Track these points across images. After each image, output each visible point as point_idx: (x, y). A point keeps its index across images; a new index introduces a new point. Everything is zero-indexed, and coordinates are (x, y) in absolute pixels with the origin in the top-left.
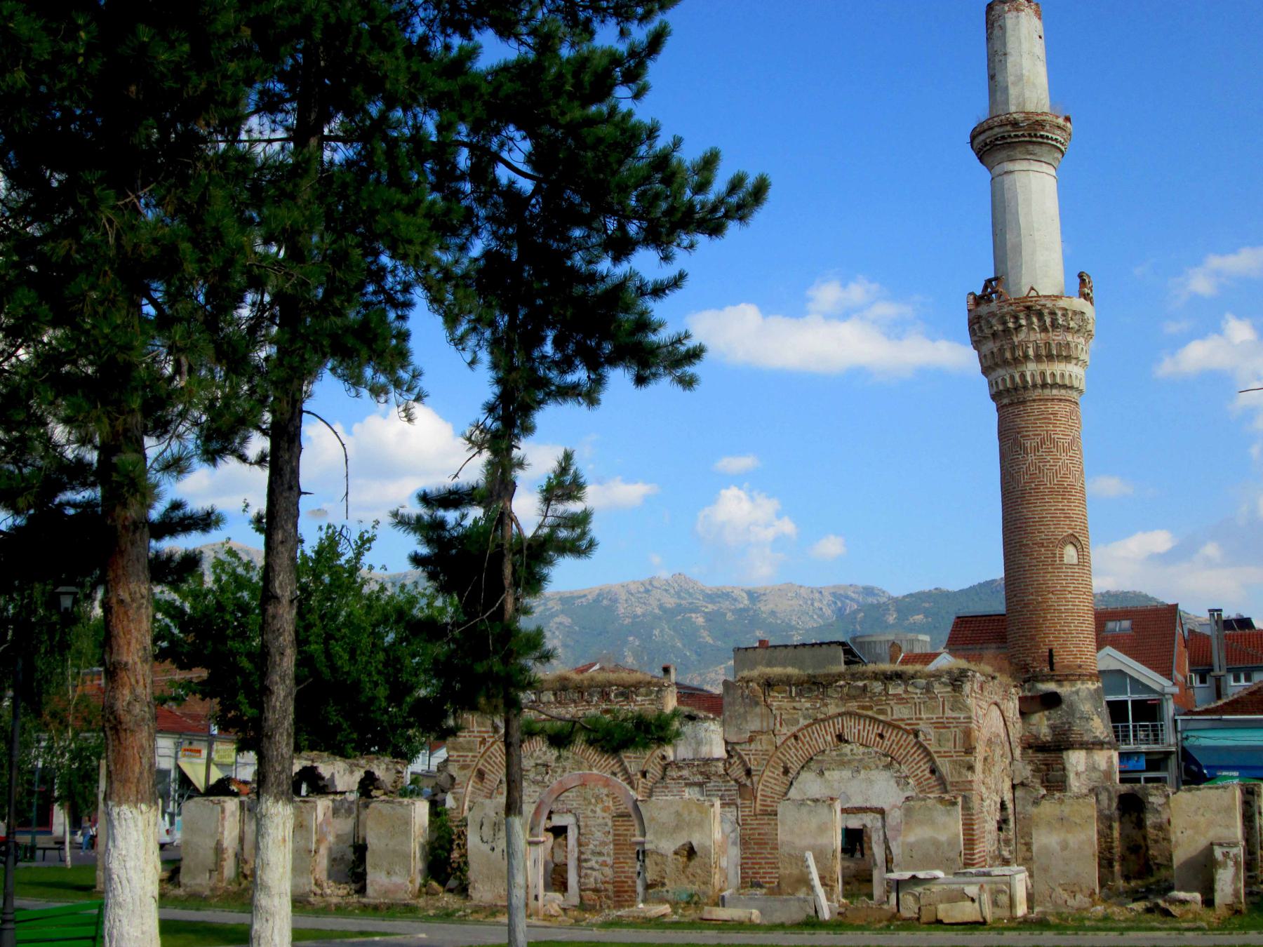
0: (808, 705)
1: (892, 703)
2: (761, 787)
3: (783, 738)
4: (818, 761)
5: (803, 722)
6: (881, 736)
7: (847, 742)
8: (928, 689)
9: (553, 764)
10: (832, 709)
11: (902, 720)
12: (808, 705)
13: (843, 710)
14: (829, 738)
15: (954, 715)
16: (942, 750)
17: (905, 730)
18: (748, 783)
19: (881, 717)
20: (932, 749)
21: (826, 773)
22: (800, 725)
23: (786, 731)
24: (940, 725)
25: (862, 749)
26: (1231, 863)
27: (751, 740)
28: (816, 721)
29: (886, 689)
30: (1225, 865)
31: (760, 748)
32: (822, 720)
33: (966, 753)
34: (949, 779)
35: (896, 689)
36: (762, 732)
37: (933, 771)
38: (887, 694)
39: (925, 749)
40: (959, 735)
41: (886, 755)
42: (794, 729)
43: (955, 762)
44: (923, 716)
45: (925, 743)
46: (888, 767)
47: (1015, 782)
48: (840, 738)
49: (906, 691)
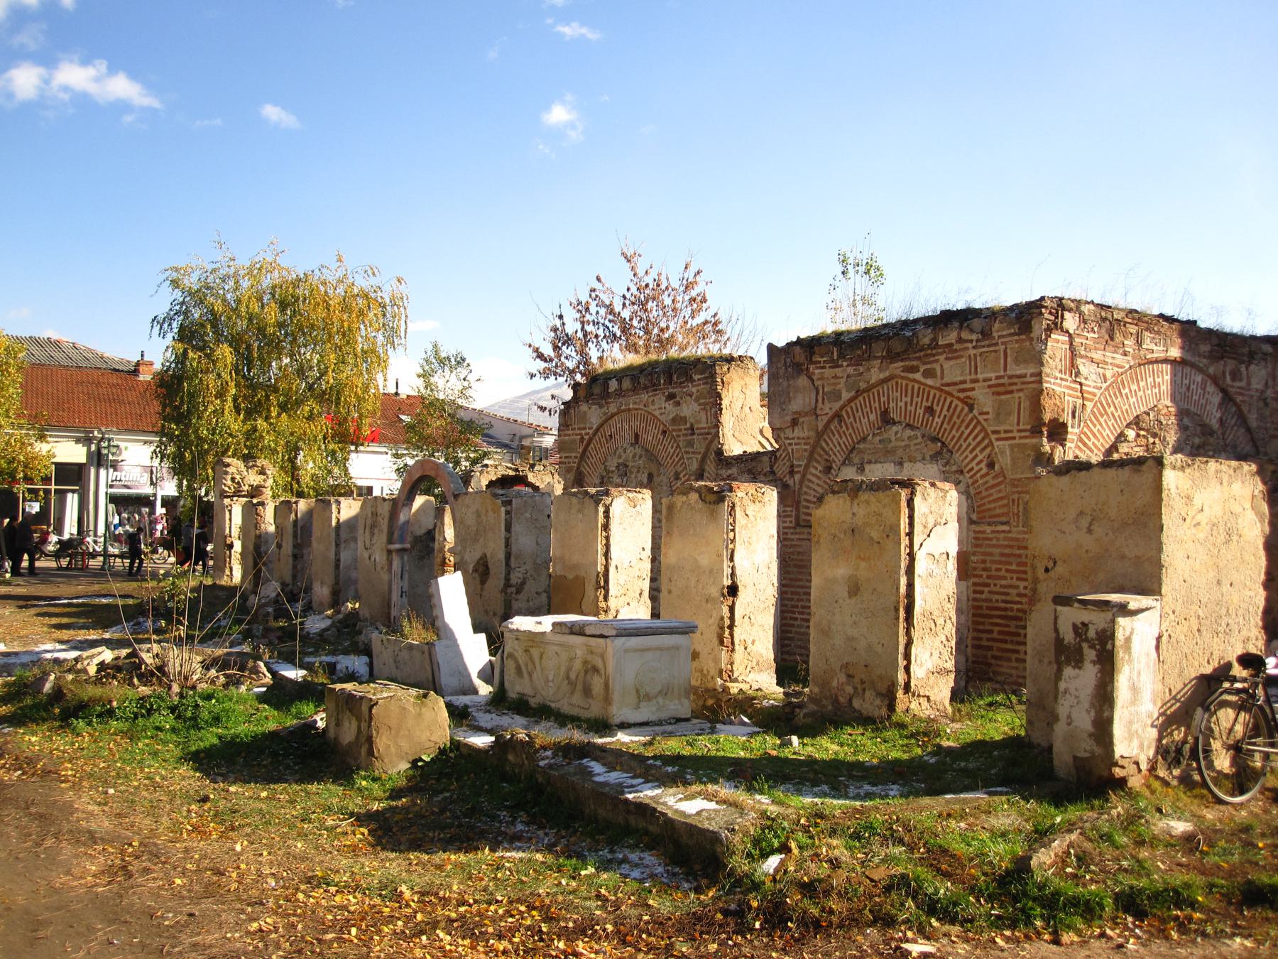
0: (850, 370)
1: (942, 358)
2: (805, 489)
3: (825, 419)
4: (861, 452)
5: (846, 396)
6: (930, 410)
7: (894, 423)
8: (986, 334)
9: (631, 464)
10: (875, 375)
11: (955, 384)
13: (887, 374)
14: (872, 417)
15: (1018, 372)
16: (1001, 428)
17: (958, 398)
18: (791, 482)
20: (989, 429)
21: (867, 467)
22: (841, 403)
23: (829, 408)
24: (1000, 389)
25: (908, 432)
26: (1090, 654)
27: (794, 423)
28: (859, 393)
29: (935, 339)
30: (1078, 662)
31: (802, 435)
32: (867, 390)
34: (1010, 476)
35: (950, 337)
36: (806, 414)
37: (991, 465)
39: (983, 429)
40: (1025, 404)
41: (935, 439)
42: (837, 406)
43: (1018, 445)
44: (980, 376)
45: (981, 418)
46: (935, 457)
49: (960, 340)
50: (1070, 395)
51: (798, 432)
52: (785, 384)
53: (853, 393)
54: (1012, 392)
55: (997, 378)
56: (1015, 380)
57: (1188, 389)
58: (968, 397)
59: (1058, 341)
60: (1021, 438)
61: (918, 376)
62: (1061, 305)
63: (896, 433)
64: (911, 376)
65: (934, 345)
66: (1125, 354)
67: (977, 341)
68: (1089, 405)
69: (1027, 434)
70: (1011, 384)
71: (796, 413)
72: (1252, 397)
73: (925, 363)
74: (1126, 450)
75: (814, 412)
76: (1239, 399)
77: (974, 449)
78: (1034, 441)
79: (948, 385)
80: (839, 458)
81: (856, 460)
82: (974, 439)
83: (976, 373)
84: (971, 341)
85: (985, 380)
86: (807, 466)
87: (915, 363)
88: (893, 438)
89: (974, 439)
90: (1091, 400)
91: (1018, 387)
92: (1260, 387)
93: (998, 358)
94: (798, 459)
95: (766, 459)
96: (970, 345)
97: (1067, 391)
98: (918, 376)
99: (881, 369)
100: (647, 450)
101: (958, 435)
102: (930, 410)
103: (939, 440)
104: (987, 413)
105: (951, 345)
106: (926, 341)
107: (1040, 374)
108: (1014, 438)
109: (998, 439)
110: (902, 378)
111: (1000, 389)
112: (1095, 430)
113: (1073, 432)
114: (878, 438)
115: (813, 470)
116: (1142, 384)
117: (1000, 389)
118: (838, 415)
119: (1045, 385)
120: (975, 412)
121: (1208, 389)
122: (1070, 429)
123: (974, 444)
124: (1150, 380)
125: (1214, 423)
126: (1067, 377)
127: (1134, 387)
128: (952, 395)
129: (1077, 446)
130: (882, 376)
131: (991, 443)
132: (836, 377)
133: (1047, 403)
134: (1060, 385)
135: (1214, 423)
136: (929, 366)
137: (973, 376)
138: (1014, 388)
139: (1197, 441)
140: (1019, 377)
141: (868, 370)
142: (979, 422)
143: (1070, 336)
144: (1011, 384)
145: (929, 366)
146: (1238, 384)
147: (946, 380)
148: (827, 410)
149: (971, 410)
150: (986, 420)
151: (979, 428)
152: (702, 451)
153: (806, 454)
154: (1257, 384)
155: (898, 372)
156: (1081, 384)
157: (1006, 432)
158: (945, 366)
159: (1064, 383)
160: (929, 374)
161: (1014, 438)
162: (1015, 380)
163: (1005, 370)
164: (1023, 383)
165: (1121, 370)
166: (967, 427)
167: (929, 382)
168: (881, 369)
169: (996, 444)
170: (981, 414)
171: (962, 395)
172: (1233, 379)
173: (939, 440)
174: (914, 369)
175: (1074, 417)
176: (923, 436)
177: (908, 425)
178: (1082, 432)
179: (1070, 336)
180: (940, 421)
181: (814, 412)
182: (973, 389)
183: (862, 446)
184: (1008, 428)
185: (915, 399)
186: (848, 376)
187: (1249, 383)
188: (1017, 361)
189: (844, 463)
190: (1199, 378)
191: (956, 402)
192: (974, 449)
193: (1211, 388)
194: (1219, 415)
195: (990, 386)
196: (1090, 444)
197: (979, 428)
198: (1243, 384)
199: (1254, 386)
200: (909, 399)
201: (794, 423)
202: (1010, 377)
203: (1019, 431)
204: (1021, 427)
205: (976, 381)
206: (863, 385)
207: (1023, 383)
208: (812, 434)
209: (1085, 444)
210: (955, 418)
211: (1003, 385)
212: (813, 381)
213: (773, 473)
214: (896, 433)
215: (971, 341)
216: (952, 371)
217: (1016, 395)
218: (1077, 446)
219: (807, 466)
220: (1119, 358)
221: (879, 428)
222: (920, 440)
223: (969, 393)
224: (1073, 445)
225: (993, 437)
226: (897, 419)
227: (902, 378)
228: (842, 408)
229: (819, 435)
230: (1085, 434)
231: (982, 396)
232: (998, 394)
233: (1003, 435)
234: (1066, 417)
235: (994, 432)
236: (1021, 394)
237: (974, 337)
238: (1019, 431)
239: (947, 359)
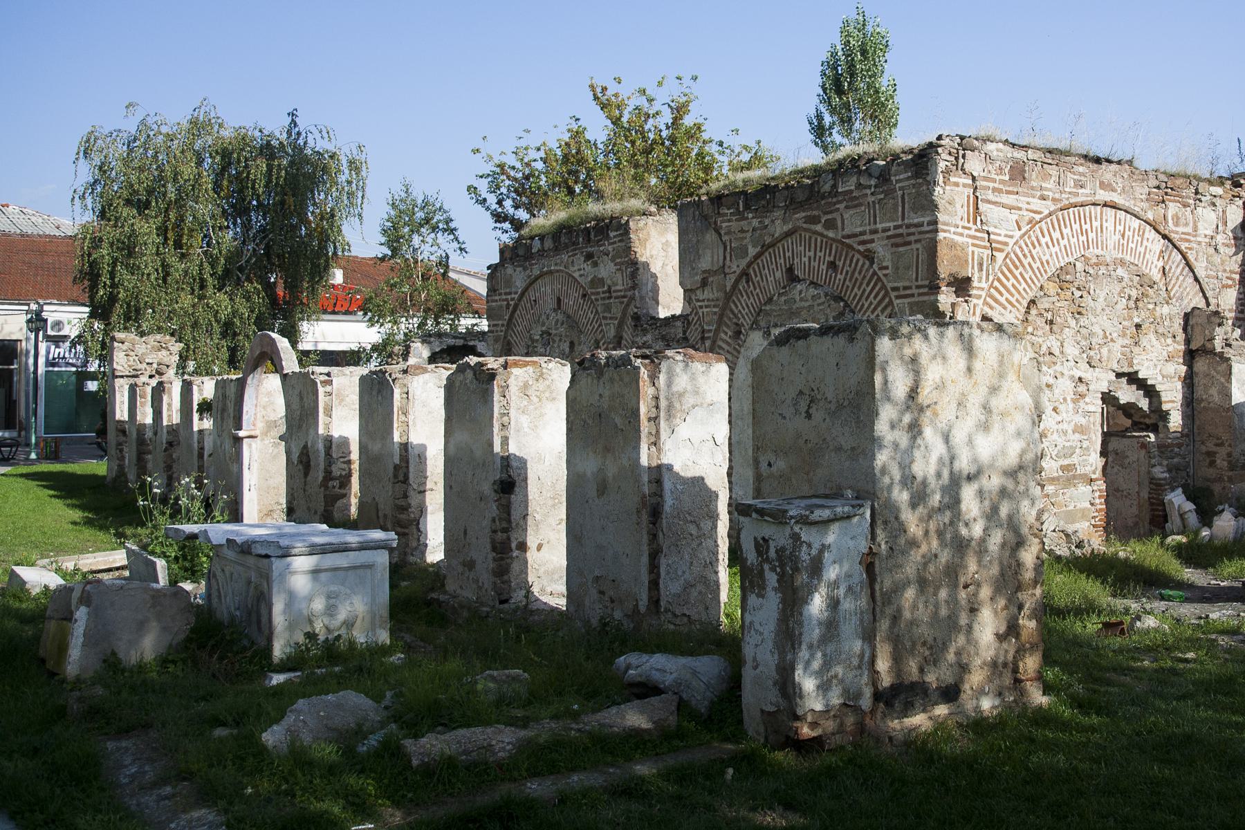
0: (755, 223)
3: (733, 278)
4: (768, 314)
5: (752, 252)
6: (832, 265)
7: (799, 281)
10: (779, 228)
11: (855, 235)
12: (755, 223)
14: (778, 274)
15: (916, 221)
17: (859, 251)
19: (831, 234)
20: (889, 286)
23: (736, 266)
24: (898, 241)
25: (812, 292)
28: (765, 247)
29: (834, 186)
32: (772, 245)
33: (931, 288)
35: (849, 185)
38: (837, 194)
39: (884, 287)
41: (838, 299)
42: (743, 263)
45: (880, 273)
47: (1193, 347)
48: (792, 277)
49: (859, 186)
50: (973, 245)
51: (707, 294)
52: (694, 240)
53: (758, 249)
54: (909, 243)
55: (896, 227)
56: (912, 230)
57: (1123, 236)
58: (868, 250)
59: (957, 184)
60: (920, 295)
61: (819, 228)
62: (964, 145)
63: (801, 292)
64: (812, 227)
65: (834, 192)
66: (1043, 198)
67: (876, 186)
68: (1000, 256)
69: (926, 290)
70: (909, 234)
71: (704, 272)
72: (1199, 243)
73: (825, 213)
74: (1047, 306)
75: (722, 270)
76: (1183, 246)
77: (875, 309)
78: (932, 298)
79: (849, 237)
80: (746, 322)
81: (763, 324)
82: (875, 297)
83: (875, 223)
84: (870, 187)
85: (885, 230)
86: (717, 331)
87: (816, 213)
88: (798, 298)
89: (875, 297)
90: (1002, 251)
91: (917, 237)
92: (1209, 232)
93: (896, 205)
94: (709, 324)
95: (679, 324)
96: (868, 192)
97: (970, 241)
98: (819, 228)
99: (784, 221)
100: (569, 317)
101: (859, 293)
102: (832, 265)
103: (842, 300)
104: (887, 268)
105: (851, 191)
106: (827, 187)
107: (935, 222)
108: (913, 295)
109: (897, 297)
110: (806, 230)
111: (899, 240)
112: (1009, 285)
113: (980, 284)
114: (783, 298)
115: (723, 335)
116: (1066, 231)
117: (899, 240)
118: (745, 274)
119: (941, 235)
120: (875, 266)
121: (1146, 235)
122: (975, 284)
123: (875, 302)
124: (1076, 227)
125: (1156, 275)
126: (971, 225)
127: (1056, 235)
128: (853, 249)
129: (985, 303)
130: (785, 228)
131: (891, 303)
132: (742, 231)
133: (943, 253)
134: (962, 235)
135: (1156, 275)
136: (829, 217)
137: (873, 227)
138: (912, 238)
139: (1134, 293)
140: (916, 226)
141: (773, 221)
142: (879, 279)
143: (974, 179)
144: (909, 234)
145: (829, 217)
146: (1180, 229)
147: (847, 232)
148: (734, 268)
149: (872, 263)
150: (885, 275)
151: (879, 285)
152: (619, 315)
153: (715, 317)
154: (1206, 229)
155: (801, 223)
156: (988, 233)
157: (905, 288)
158: (846, 216)
159: (966, 232)
160: (830, 225)
161: (913, 295)
162: (912, 230)
163: (903, 219)
164: (920, 233)
165: (1037, 217)
166: (868, 285)
167: (831, 234)
168: (784, 221)
169: (896, 302)
170: (880, 269)
171: (861, 248)
172: (1177, 224)
173: (842, 300)
174: (814, 220)
175: (981, 270)
176: (826, 295)
177: (812, 283)
178: (991, 286)
179: (974, 179)
180: (842, 277)
181: (722, 270)
182: (872, 241)
183: (768, 308)
184: (907, 284)
185: (818, 254)
186: (754, 230)
187: (1195, 229)
188: (915, 209)
189: (751, 328)
190: (1136, 223)
191: (857, 256)
192: (875, 309)
193: (1150, 234)
194: (1161, 264)
195: (889, 237)
196: (1002, 300)
197: (879, 285)
198: (1189, 229)
199: (1201, 231)
200: (812, 254)
201: (704, 283)
202: (908, 226)
203: (918, 287)
204: (920, 283)
205: (875, 232)
206: (768, 240)
207: (920, 233)
208: (720, 295)
209: (996, 301)
210: (856, 274)
211: (901, 235)
212: (720, 235)
213: (686, 339)
214: (801, 292)
215: (870, 187)
216: (852, 222)
217: (914, 246)
218: (985, 303)
219: (717, 331)
220: (1036, 204)
221: (784, 287)
222: (823, 299)
223: (869, 246)
224: (980, 302)
225: (893, 294)
226: (801, 277)
227: (806, 230)
228: (749, 265)
229: (728, 297)
230: (996, 289)
231: (881, 249)
232: (897, 245)
233: (902, 293)
234: (971, 271)
235: (894, 289)
236: (918, 246)
237: (873, 182)
238: (918, 287)
239: (847, 207)
